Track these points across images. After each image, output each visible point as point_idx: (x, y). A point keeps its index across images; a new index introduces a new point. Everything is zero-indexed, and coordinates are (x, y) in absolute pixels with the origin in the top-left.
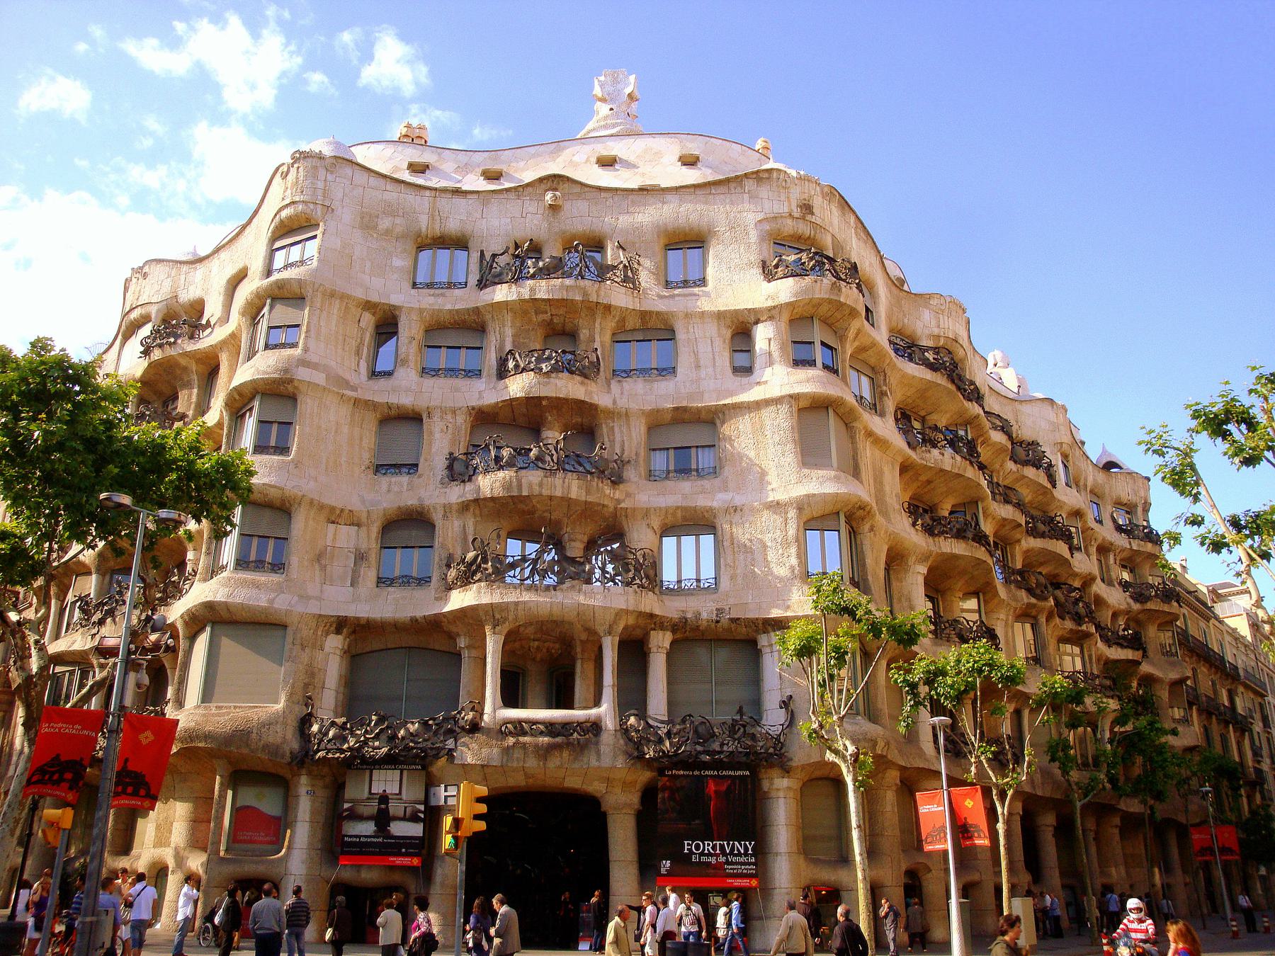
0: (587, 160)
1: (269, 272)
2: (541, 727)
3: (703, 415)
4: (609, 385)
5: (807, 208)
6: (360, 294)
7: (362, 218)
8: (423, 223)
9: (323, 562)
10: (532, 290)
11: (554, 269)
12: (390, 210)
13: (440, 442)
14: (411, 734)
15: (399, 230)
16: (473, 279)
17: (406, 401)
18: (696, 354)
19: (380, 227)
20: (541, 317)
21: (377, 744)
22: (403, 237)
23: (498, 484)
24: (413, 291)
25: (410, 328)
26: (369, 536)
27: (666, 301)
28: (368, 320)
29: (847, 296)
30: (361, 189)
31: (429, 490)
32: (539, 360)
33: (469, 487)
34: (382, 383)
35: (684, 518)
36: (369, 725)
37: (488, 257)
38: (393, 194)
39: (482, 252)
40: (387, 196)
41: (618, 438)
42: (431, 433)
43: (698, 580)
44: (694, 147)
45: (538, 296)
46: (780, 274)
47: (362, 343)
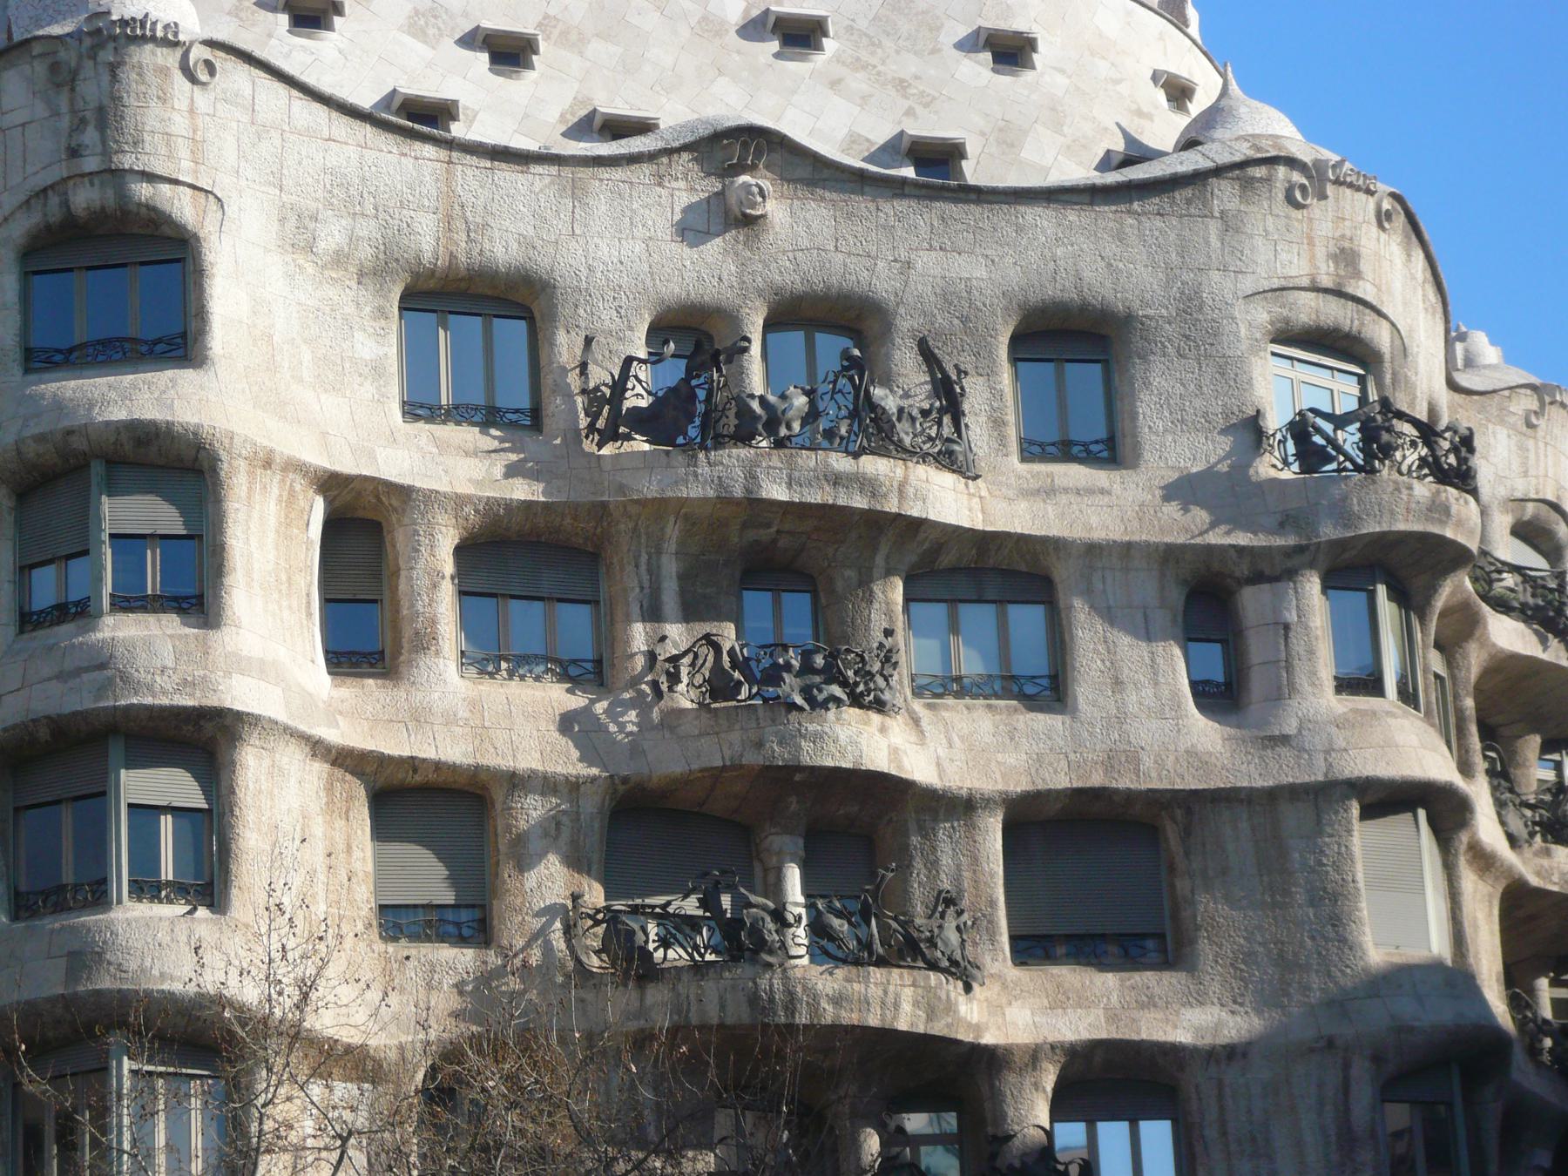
4: (916, 721)
5: (1347, 257)
7: (282, 220)
15: (366, 253)
17: (449, 747)
19: (321, 246)
20: (752, 535)
29: (1460, 524)
30: (275, 135)
33: (657, 994)
34: (368, 693)
41: (946, 861)
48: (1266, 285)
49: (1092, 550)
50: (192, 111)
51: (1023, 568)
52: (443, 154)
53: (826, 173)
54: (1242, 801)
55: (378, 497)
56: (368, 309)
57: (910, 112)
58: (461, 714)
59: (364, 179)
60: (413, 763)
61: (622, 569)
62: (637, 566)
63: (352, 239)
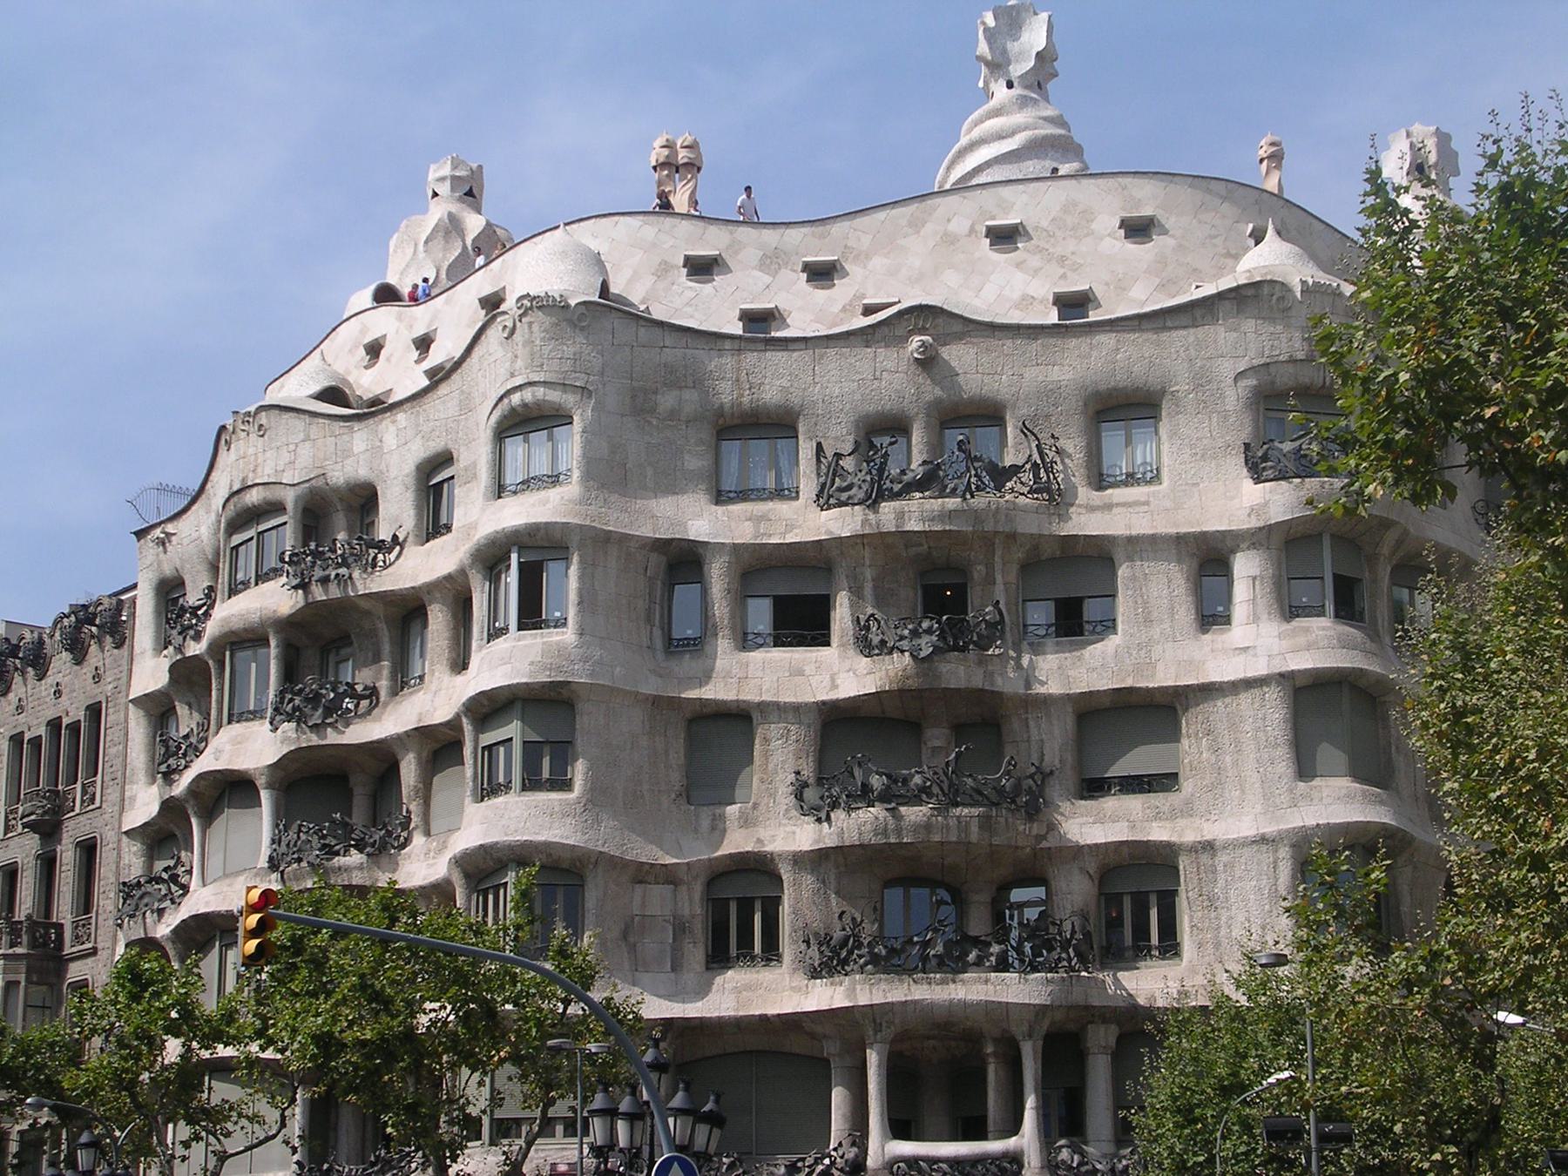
0: (972, 230)
1: (499, 490)
2: (944, 1166)
6: (646, 531)
7: (633, 397)
8: (726, 394)
9: (631, 940)
10: (900, 515)
11: (930, 481)
12: (676, 378)
16: (808, 485)
19: (660, 409)
20: (913, 551)
23: (868, 827)
24: (720, 509)
26: (691, 900)
27: (1097, 516)
28: (657, 561)
30: (627, 349)
32: (915, 634)
36: (718, 1169)
37: (829, 453)
39: (819, 445)
40: (669, 355)
42: (766, 740)
44: (1146, 199)
45: (907, 528)
48: (1256, 362)
49: (1132, 540)
52: (736, 345)
53: (971, 327)
57: (1064, 276)
59: (685, 366)
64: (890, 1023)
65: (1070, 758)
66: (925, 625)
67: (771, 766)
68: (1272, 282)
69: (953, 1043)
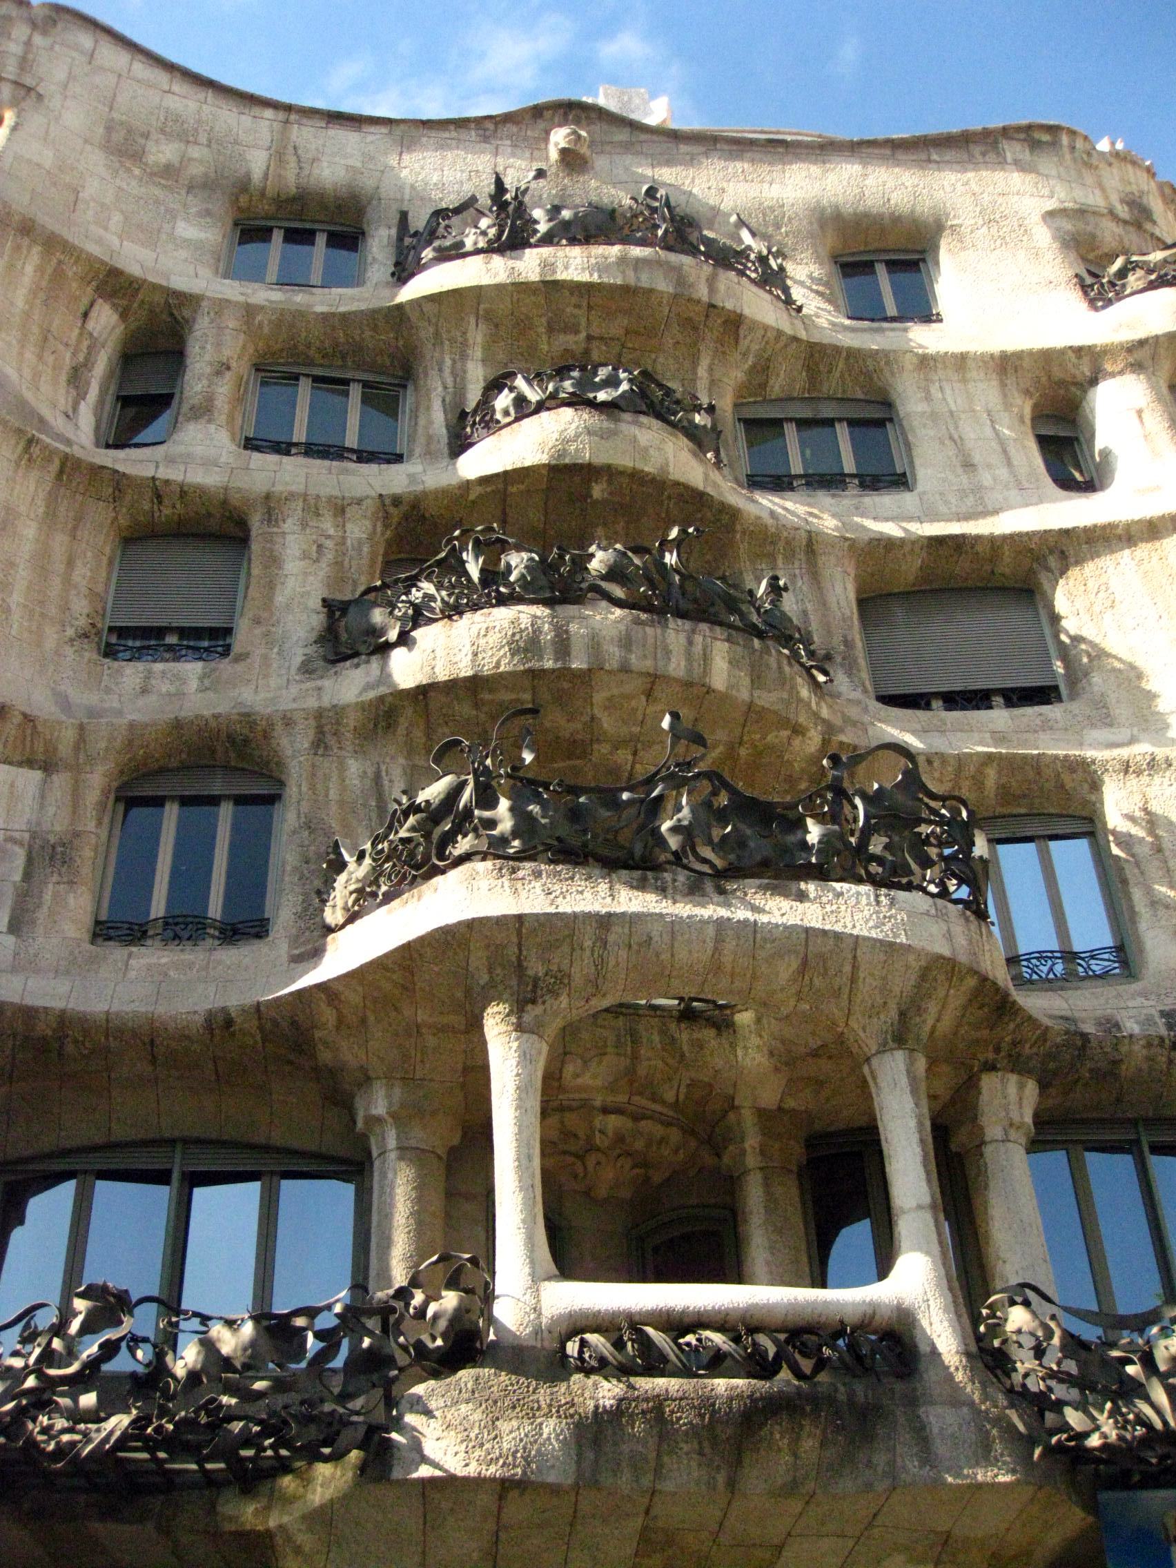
3: (1006, 565)
7: (109, 129)
8: (257, 163)
10: (546, 265)
13: (295, 581)
14: (227, 1363)
15: (196, 170)
18: (958, 442)
19: (151, 159)
21: (88, 1400)
22: (206, 185)
25: (218, 345)
28: (106, 320)
30: (112, 79)
31: (271, 680)
35: (1005, 795)
38: (186, 103)
39: (404, 216)
40: (173, 103)
42: (274, 561)
43: (1070, 956)
45: (561, 276)
46: (1141, 284)
47: (87, 364)
50: (28, 43)
51: (861, 396)
52: (281, 115)
53: (643, 137)
54: (1120, 538)
55: (172, 314)
56: (194, 210)
58: (222, 460)
59: (199, 121)
60: (157, 490)
61: (426, 375)
62: (440, 370)
63: (185, 160)
64: (561, 980)
65: (859, 645)
66: (603, 373)
67: (280, 599)
68: (1072, 133)
69: (659, 1130)
